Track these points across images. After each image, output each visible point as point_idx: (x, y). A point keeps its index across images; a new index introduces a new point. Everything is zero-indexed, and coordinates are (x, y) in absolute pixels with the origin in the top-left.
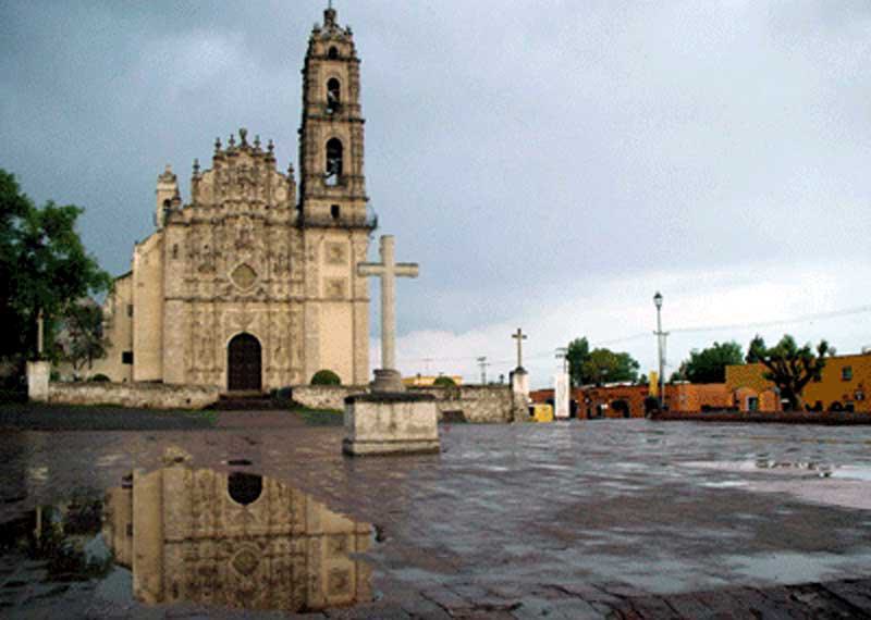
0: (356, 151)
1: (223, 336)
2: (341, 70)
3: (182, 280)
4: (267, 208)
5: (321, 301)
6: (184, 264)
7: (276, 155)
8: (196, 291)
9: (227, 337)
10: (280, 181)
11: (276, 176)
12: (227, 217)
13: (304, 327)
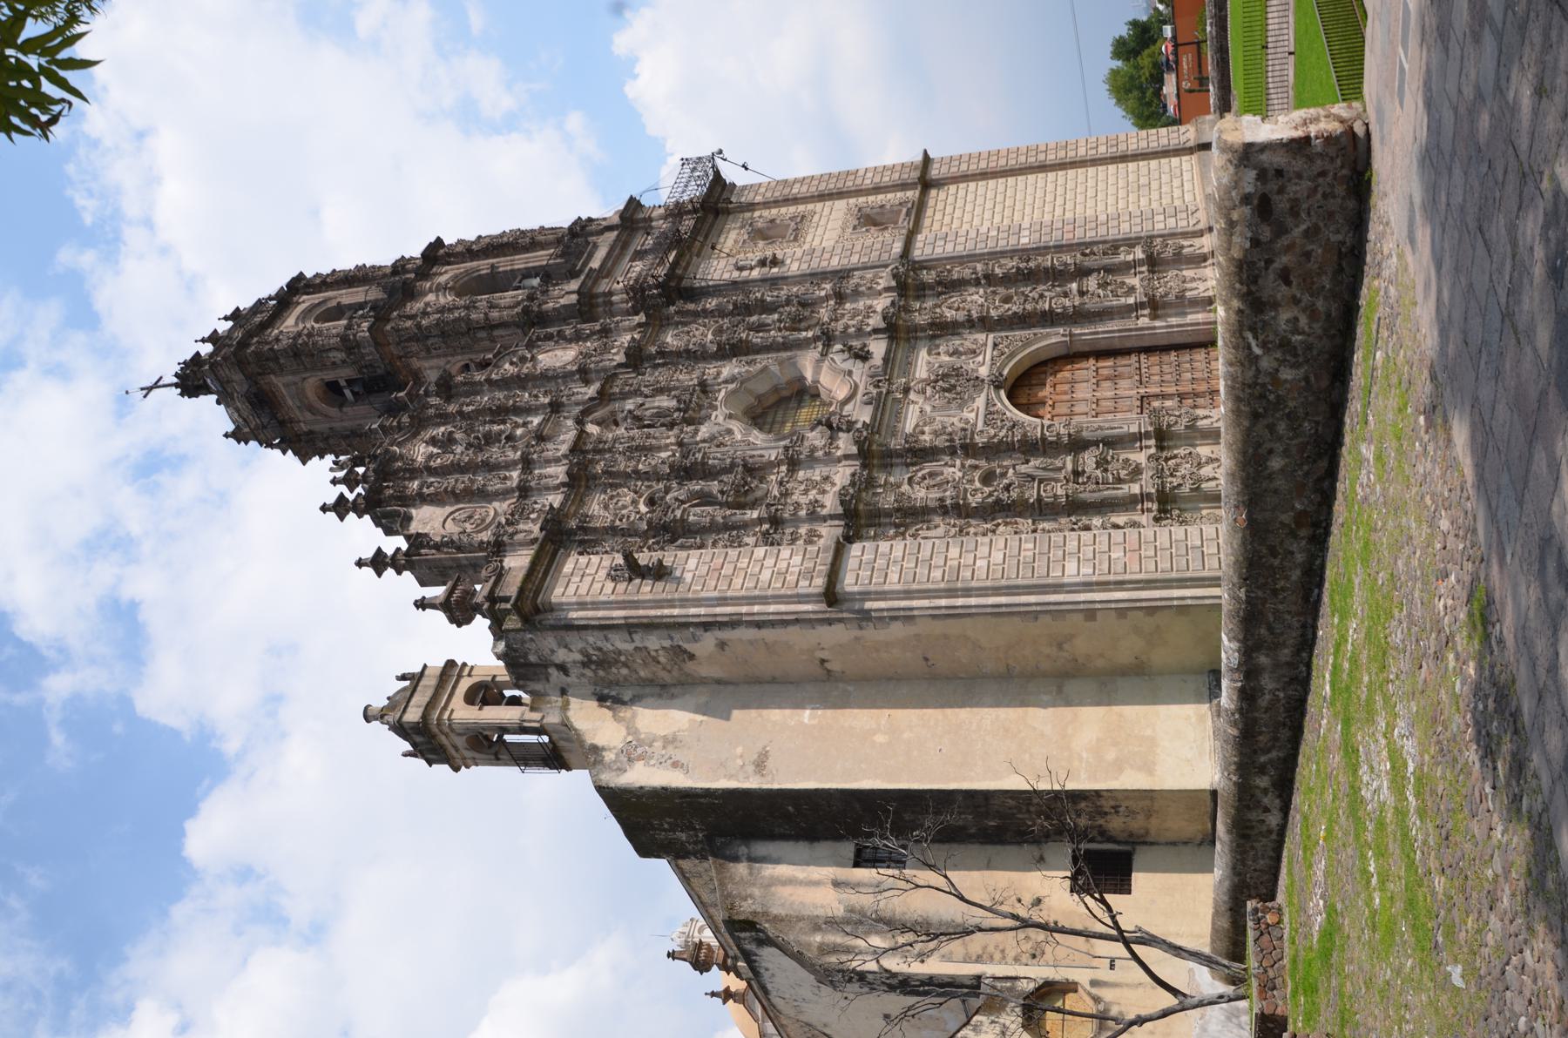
3: (760, 552)
13: (996, 255)
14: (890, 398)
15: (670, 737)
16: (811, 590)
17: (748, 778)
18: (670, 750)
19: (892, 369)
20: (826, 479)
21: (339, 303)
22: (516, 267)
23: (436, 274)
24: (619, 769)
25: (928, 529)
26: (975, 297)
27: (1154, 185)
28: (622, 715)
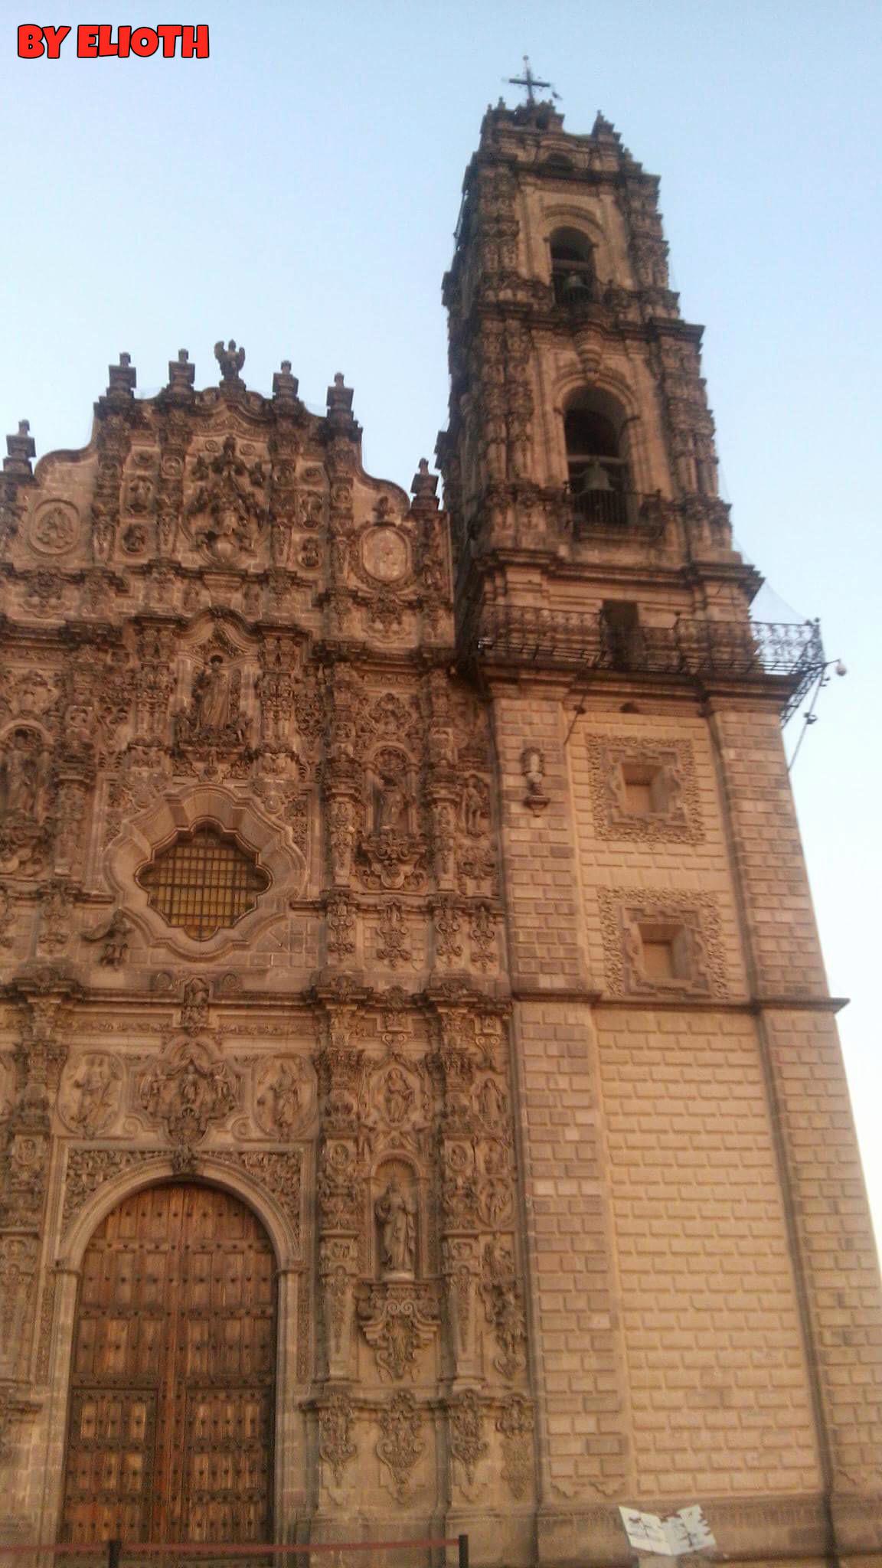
0: (682, 421)
1: (59, 1189)
2: (602, 207)
4: (322, 601)
5: (595, 1001)
7: (361, 411)
9: (79, 1195)
10: (381, 509)
12: (141, 622)
13: (515, 1139)
14: (173, 1011)
19: (238, 1007)
21: (596, 246)
22: (634, 451)
23: (626, 349)
26: (416, 1116)
27: (731, 1418)
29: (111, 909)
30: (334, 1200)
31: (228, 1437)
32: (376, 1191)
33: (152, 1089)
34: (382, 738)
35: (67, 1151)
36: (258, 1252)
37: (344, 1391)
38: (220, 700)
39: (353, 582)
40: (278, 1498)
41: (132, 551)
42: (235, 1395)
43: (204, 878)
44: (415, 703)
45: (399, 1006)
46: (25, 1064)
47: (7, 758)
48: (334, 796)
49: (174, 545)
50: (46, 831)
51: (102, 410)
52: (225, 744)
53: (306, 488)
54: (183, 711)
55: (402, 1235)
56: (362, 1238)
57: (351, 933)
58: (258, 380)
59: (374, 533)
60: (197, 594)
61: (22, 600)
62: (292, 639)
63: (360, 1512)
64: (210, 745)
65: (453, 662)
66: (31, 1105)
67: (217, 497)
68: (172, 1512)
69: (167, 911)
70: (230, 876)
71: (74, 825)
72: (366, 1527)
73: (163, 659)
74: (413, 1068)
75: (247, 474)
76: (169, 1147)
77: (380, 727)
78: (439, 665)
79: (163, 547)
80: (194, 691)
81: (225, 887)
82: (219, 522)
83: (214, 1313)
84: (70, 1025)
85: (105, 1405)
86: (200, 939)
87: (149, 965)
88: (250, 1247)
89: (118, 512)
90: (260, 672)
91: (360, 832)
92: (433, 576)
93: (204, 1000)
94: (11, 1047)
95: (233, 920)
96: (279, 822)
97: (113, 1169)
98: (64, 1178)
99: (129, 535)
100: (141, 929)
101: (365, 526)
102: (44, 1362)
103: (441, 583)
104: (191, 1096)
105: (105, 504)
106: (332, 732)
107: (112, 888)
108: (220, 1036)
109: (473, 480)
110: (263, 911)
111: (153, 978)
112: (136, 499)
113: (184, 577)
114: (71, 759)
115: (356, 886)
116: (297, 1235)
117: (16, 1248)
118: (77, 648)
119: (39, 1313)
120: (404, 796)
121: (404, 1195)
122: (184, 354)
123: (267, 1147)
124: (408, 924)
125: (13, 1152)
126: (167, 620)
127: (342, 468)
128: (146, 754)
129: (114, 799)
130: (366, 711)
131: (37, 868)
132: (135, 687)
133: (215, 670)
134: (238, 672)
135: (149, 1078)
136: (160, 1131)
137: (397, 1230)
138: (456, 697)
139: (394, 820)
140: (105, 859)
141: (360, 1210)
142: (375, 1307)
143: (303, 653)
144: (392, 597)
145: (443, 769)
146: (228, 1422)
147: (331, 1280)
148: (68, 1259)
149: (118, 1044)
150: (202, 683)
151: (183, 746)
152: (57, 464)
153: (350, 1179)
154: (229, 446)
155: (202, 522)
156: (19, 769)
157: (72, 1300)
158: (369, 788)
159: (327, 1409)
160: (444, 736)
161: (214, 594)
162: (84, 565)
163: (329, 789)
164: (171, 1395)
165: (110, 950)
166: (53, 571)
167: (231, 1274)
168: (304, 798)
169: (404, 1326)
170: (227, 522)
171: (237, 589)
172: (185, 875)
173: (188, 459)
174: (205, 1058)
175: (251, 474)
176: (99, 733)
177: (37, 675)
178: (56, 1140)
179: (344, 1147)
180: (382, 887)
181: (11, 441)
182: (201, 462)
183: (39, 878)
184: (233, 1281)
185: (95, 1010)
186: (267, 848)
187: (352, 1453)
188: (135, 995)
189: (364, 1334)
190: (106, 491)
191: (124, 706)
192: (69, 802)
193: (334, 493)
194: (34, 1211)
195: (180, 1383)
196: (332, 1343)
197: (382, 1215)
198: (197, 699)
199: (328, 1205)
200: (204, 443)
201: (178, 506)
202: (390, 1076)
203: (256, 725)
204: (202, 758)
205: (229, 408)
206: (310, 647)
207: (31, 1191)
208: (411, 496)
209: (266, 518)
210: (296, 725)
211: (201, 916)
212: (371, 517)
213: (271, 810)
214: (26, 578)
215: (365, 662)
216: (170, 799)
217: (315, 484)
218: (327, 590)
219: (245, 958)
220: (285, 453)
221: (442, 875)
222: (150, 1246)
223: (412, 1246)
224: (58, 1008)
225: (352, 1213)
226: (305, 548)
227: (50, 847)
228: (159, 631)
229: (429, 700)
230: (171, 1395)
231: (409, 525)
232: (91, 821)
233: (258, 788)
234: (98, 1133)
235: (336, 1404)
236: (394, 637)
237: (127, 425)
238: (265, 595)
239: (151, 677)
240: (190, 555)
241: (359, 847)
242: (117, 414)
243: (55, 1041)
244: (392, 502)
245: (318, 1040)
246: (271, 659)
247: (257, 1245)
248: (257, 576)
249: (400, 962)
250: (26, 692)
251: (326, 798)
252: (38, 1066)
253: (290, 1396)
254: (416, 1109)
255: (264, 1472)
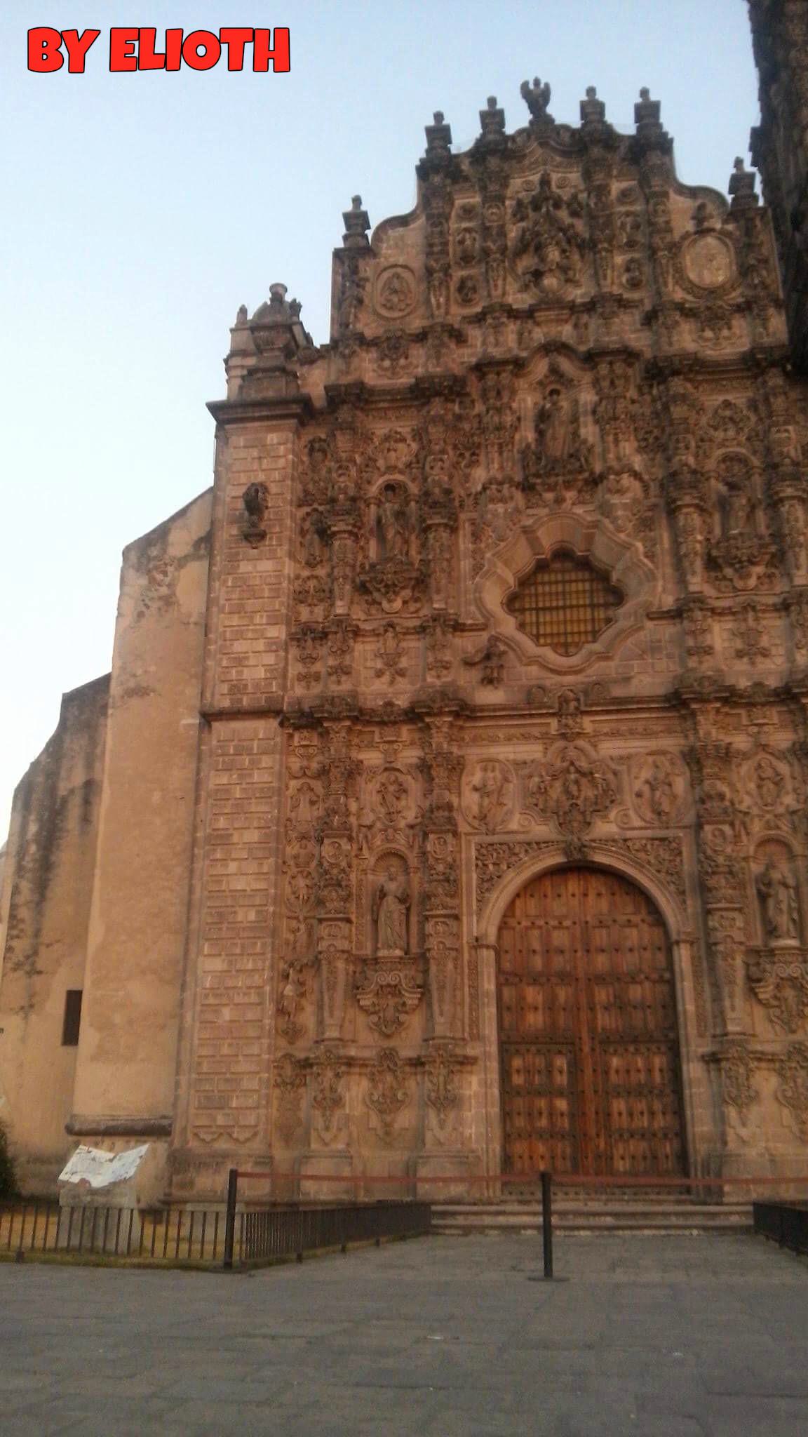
1: (470, 878)
3: (278, 632)
4: (649, 319)
6: (289, 568)
8: (343, 671)
9: (488, 882)
10: (700, 217)
11: (678, 203)
12: (481, 368)
15: (174, 599)
16: (217, 697)
17: (122, 684)
18: (155, 605)
20: (402, 673)
24: (140, 563)
25: (312, 803)
28: (203, 546)
29: (485, 636)
30: (716, 877)
31: (640, 1084)
32: (756, 868)
33: (540, 788)
34: (722, 445)
35: (473, 846)
36: (651, 925)
37: (740, 1044)
38: (561, 431)
39: (679, 295)
40: (690, 1137)
41: (467, 301)
42: (643, 1048)
43: (564, 599)
44: (753, 405)
45: (763, 699)
46: (429, 773)
47: (381, 511)
48: (679, 507)
49: (504, 289)
50: (422, 573)
51: (424, 171)
52: (570, 472)
53: (623, 209)
54: (528, 446)
55: (784, 906)
56: (746, 910)
57: (708, 636)
58: (566, 112)
59: (695, 241)
60: (530, 332)
61: (375, 366)
62: (625, 361)
63: (767, 1149)
64: (557, 475)
65: (787, 359)
66: (438, 808)
67: (538, 234)
68: (598, 1147)
69: (534, 632)
70: (587, 595)
71: (445, 564)
72: (772, 1161)
73: (505, 400)
74: (781, 756)
75: (564, 206)
76: (560, 838)
77: (719, 435)
78: (773, 364)
79: (494, 293)
80: (537, 427)
81: (584, 606)
82: (543, 260)
83: (614, 978)
84: (463, 739)
85: (530, 1058)
86: (567, 655)
87: (524, 681)
88: (643, 921)
89: (449, 266)
90: (596, 398)
91: (708, 540)
92: (759, 275)
93: (577, 708)
94: (415, 761)
95: (595, 635)
96: (627, 539)
97: (514, 858)
98: (474, 868)
99: (461, 287)
100: (514, 650)
101: (686, 236)
102: (475, 1022)
103: (768, 281)
104: (576, 793)
105: (436, 261)
106: (671, 446)
107: (484, 616)
108: (594, 739)
109: (792, 168)
110: (622, 624)
111: (529, 693)
112: (464, 251)
113: (516, 318)
114: (435, 504)
115: (709, 591)
116: (685, 910)
117: (440, 928)
118: (428, 403)
119: (466, 981)
120: (749, 500)
121: (783, 870)
122: (492, 101)
123: (649, 833)
124: (764, 622)
125: (429, 848)
126: (504, 363)
127: (656, 182)
128: (499, 491)
129: (476, 537)
130: (704, 421)
131: (418, 605)
132: (483, 430)
133: (554, 404)
134: (576, 402)
135: (536, 779)
136: (551, 824)
137: (778, 902)
138: (794, 394)
139: (741, 523)
140: (475, 591)
141: (742, 886)
142: (765, 971)
143: (636, 372)
144: (720, 303)
145: (787, 468)
146: (639, 1071)
147: (721, 948)
148: (486, 935)
149: (506, 752)
150: (543, 417)
151: (532, 480)
152: (390, 232)
153: (729, 858)
154: (545, 182)
155: (527, 262)
156: (392, 520)
157: (493, 970)
158: (714, 497)
159: (727, 1059)
160: (786, 434)
161: (545, 330)
162: (426, 323)
163: (674, 501)
164: (586, 1049)
165: (489, 671)
166: (399, 333)
167: (629, 944)
168: (649, 514)
169: (794, 987)
170: (551, 256)
171: (566, 321)
172: (547, 598)
173: (507, 203)
174: (583, 758)
175: (569, 205)
176: (456, 480)
177: (396, 432)
178: (463, 837)
179: (721, 830)
180: (734, 588)
181: (347, 217)
182: (520, 203)
183: (421, 614)
184: (631, 950)
185: (482, 724)
186: (620, 566)
187: (755, 1098)
188: (513, 709)
189: (756, 994)
190: (436, 249)
191: (474, 450)
192: (438, 544)
193: (651, 207)
194: (452, 896)
195: (593, 1038)
196: (727, 1003)
197: (763, 888)
198: (540, 433)
199: (711, 882)
200: (520, 184)
201: (503, 250)
202: (760, 766)
203: (598, 449)
204: (551, 488)
205: (541, 145)
206: (643, 366)
207: (448, 880)
208: (729, 198)
209: (587, 247)
210: (636, 444)
211: (566, 634)
212: (690, 226)
213: (619, 530)
214: (376, 345)
215: (698, 372)
216: (526, 531)
217: (631, 203)
218: (654, 307)
219: (611, 668)
220: (599, 178)
221: (794, 571)
222: (553, 923)
223: (795, 916)
224: (451, 725)
225: (734, 888)
226: (628, 270)
227: (427, 587)
228: (498, 374)
229: (766, 400)
230: (586, 1049)
231: (730, 227)
232: (459, 560)
233: (606, 510)
234: (498, 828)
235: (736, 1055)
236: (724, 343)
237: (448, 181)
238: (594, 322)
239: (496, 419)
240: (519, 296)
241: (709, 555)
242: (437, 172)
243: (451, 753)
244: (710, 208)
245: (686, 737)
246: (605, 384)
247: (649, 919)
248: (584, 304)
249: (759, 659)
250: (389, 450)
251: (672, 511)
252: (440, 774)
253: (693, 1048)
254: (787, 793)
255: (675, 1113)
